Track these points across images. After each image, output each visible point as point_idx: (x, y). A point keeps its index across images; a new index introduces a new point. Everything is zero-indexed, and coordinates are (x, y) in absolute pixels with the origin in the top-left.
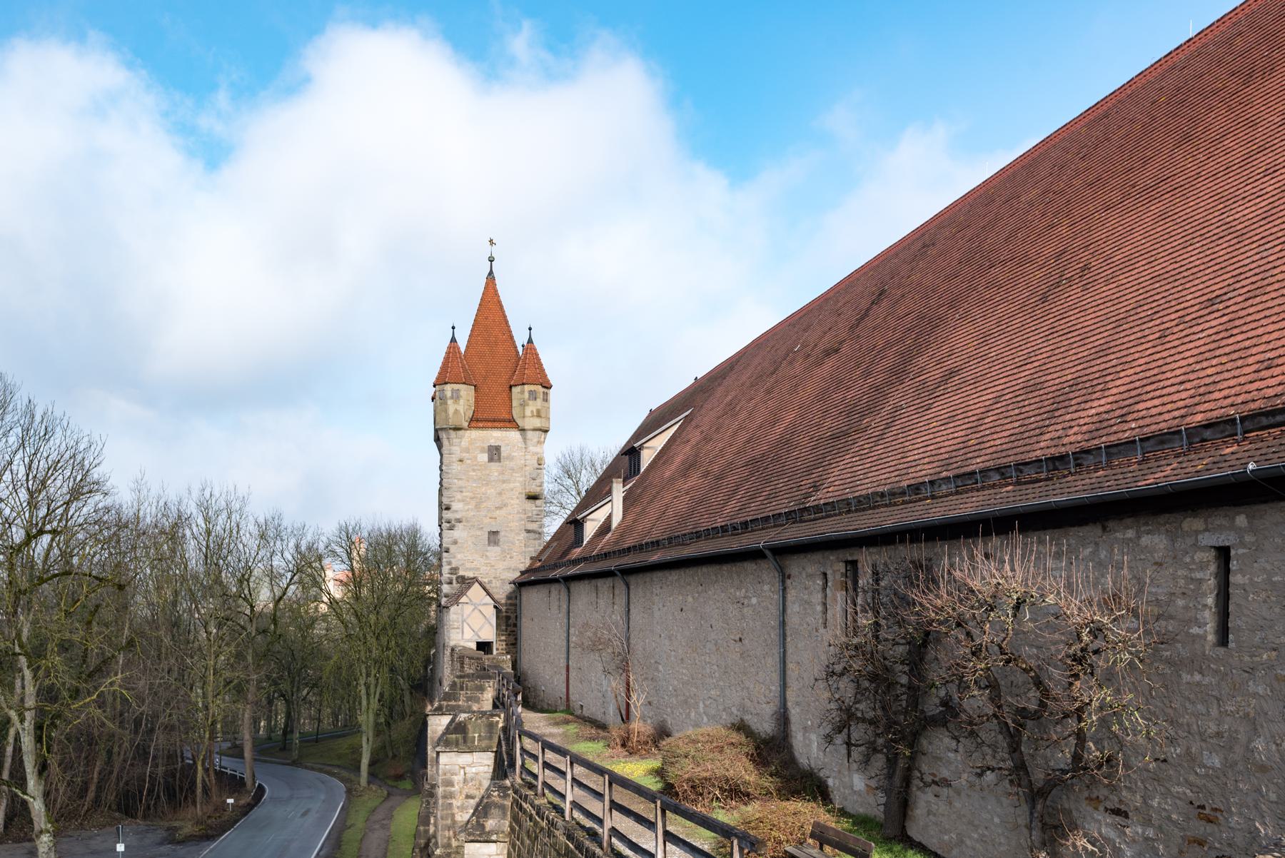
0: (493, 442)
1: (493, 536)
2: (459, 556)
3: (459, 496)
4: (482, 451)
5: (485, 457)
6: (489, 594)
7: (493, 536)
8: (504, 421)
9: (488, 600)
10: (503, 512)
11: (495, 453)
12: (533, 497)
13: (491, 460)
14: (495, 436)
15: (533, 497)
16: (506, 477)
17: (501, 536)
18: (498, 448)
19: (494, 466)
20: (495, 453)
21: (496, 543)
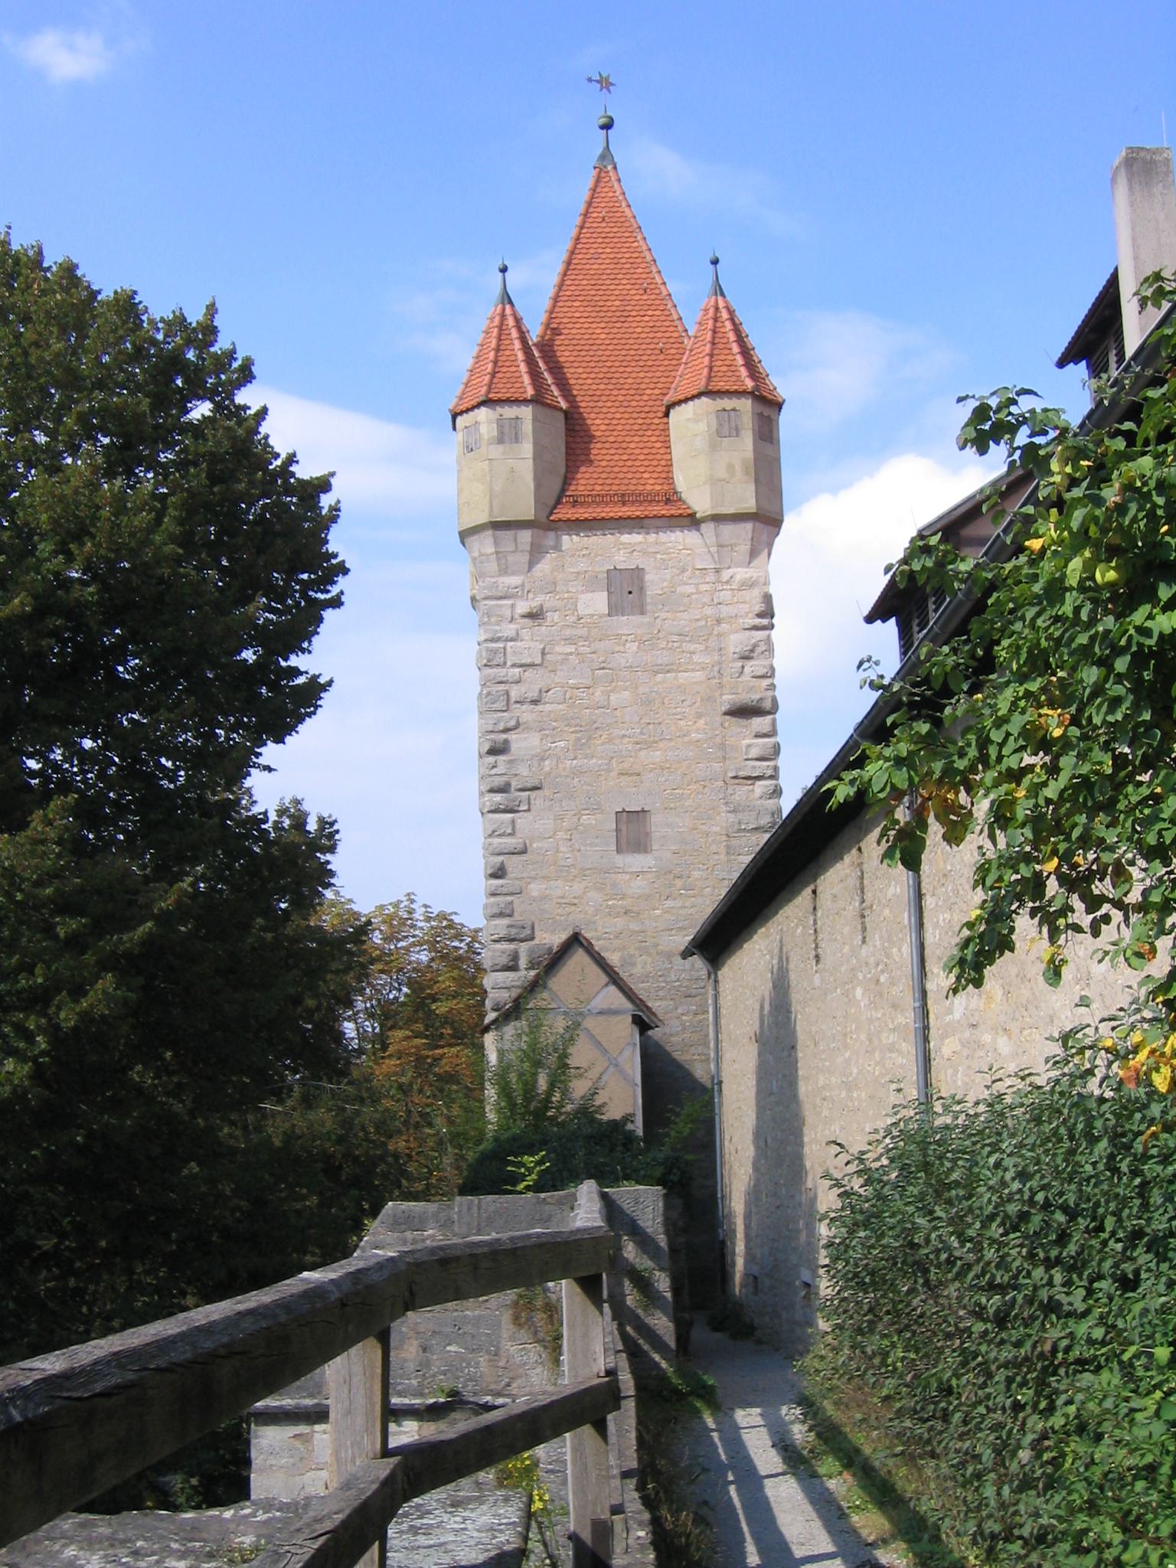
0: (622, 560)
1: (632, 830)
2: (535, 889)
3: (526, 714)
4: (591, 585)
5: (597, 602)
6: (614, 978)
7: (632, 830)
8: (650, 499)
9: (613, 997)
10: (657, 755)
11: (627, 590)
12: (744, 712)
13: (614, 609)
14: (623, 548)
15: (744, 712)
16: (663, 658)
17: (659, 825)
18: (638, 573)
19: (627, 624)
20: (627, 590)
21: (640, 845)
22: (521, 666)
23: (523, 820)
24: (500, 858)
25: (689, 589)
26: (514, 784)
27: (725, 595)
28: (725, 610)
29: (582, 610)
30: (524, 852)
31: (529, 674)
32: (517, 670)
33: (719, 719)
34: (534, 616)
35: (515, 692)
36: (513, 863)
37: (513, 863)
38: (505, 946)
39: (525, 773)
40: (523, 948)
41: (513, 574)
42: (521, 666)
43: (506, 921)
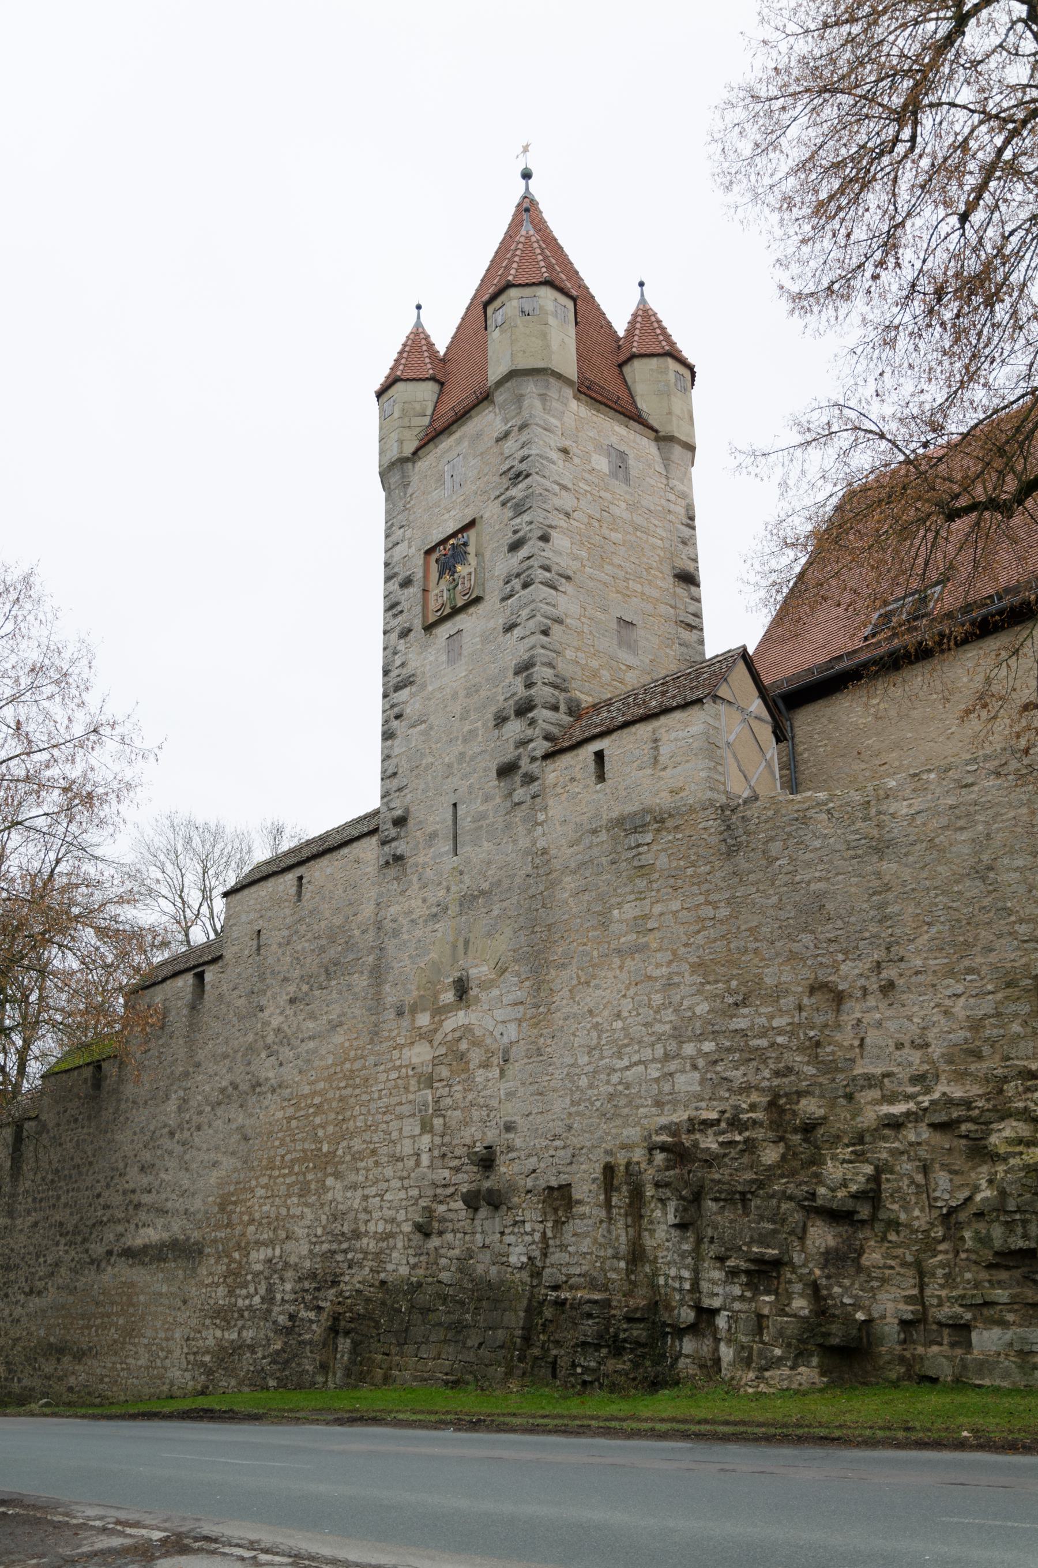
2: (569, 654)
16: (639, 520)
22: (559, 484)
23: (561, 600)
24: (549, 622)
25: (653, 482)
26: (555, 568)
27: (672, 497)
28: (672, 507)
29: (594, 464)
30: (559, 621)
31: (563, 493)
32: (557, 488)
33: (671, 579)
34: (565, 451)
35: (557, 502)
36: (556, 629)
37: (556, 629)
38: (551, 690)
39: (563, 563)
40: (562, 696)
41: (553, 416)
42: (559, 484)
43: (551, 671)
